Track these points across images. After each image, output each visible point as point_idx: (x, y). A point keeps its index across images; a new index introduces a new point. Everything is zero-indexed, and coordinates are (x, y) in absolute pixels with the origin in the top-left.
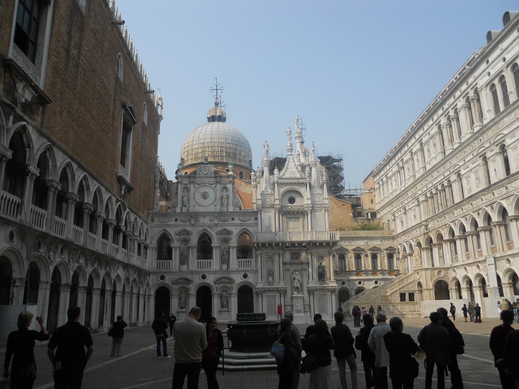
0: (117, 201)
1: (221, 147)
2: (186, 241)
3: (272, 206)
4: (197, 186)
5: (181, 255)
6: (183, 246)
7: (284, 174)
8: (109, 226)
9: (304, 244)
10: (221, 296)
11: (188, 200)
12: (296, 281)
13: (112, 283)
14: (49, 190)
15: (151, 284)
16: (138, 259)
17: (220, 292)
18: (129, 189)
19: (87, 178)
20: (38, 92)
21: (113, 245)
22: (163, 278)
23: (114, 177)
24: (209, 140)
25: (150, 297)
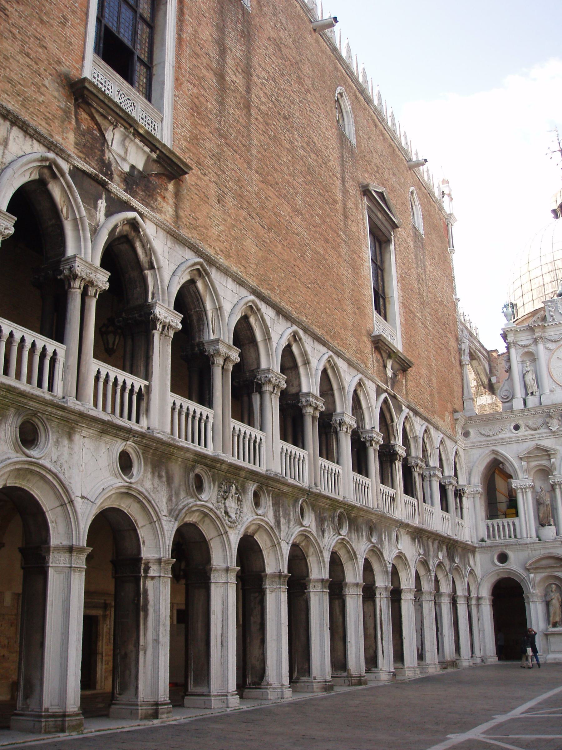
4: (551, 346)
5: (538, 503)
6: (538, 485)
8: (368, 444)
11: (538, 380)
13: (387, 572)
14: (213, 363)
15: (479, 572)
16: (443, 518)
18: (404, 366)
19: (300, 339)
20: (157, 148)
21: (382, 486)
22: (503, 558)
23: (365, 339)
25: (482, 602)
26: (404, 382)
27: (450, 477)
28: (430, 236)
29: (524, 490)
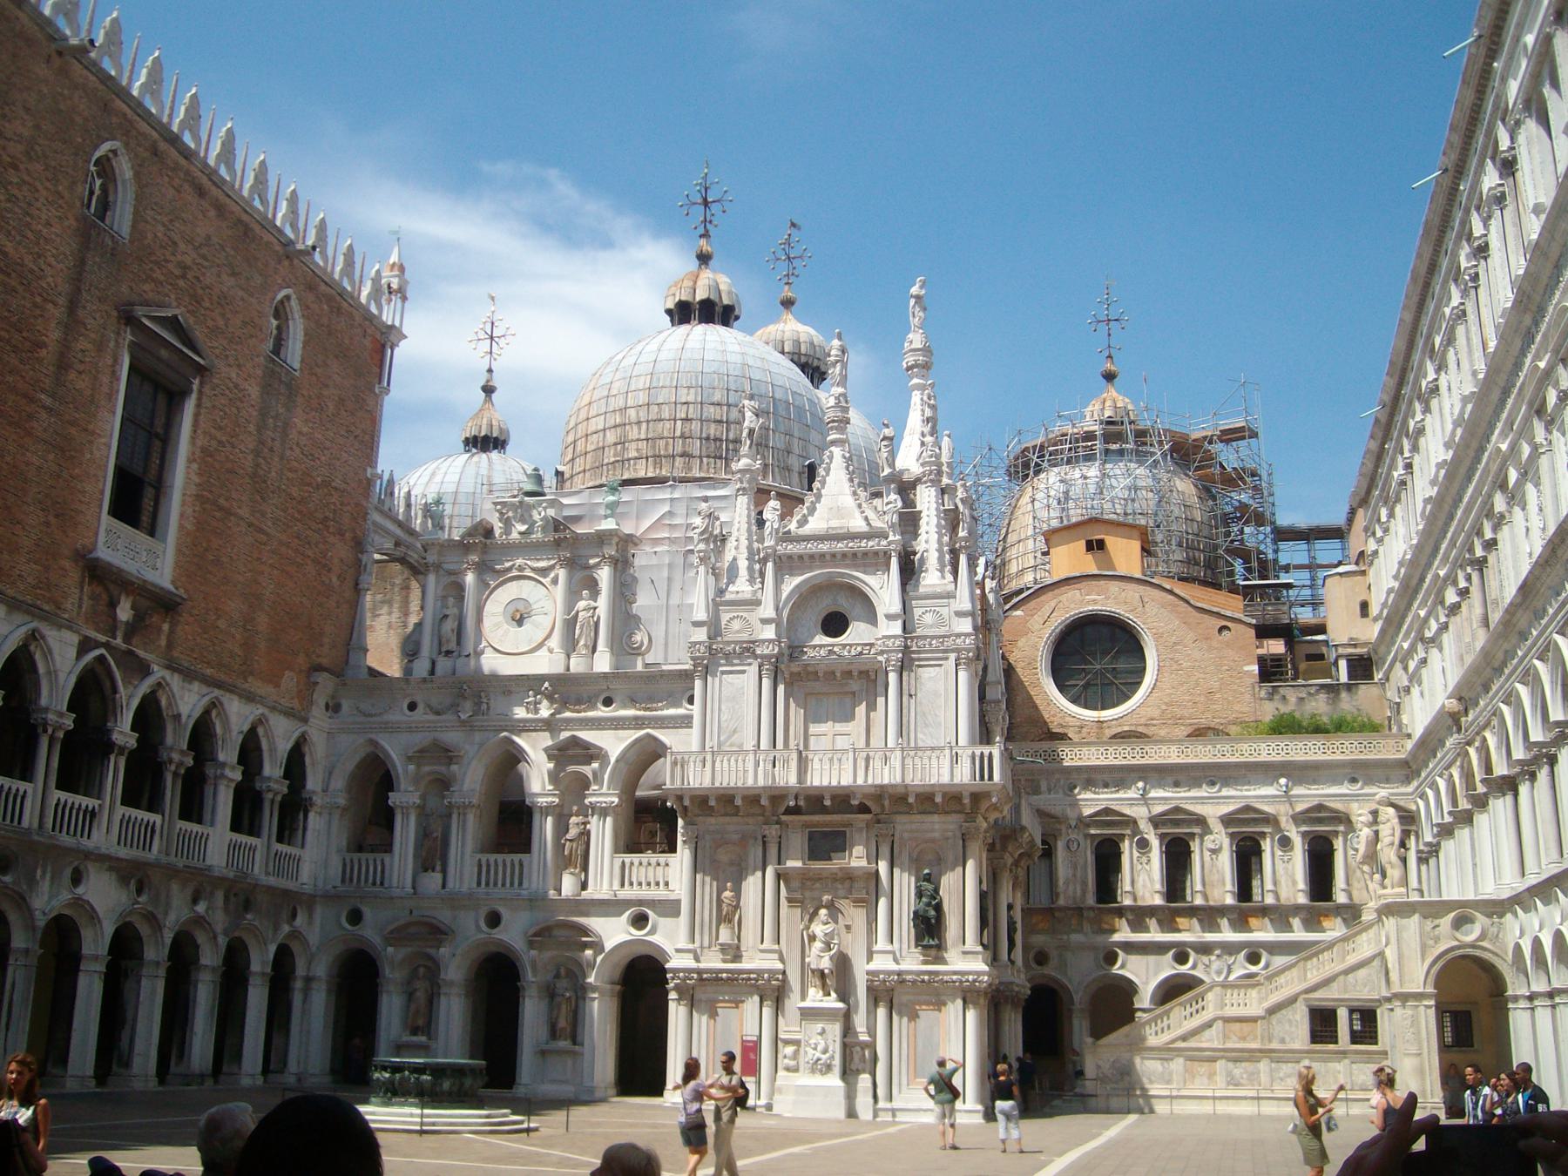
0: (85, 646)
1: (687, 419)
2: (444, 784)
3: (748, 650)
5: (424, 834)
7: (803, 522)
9: (855, 802)
10: (551, 994)
12: (818, 945)
15: (314, 937)
17: (549, 977)
18: (161, 604)
22: (356, 917)
23: (67, 564)
24: (643, 398)
25: (314, 985)
26: (166, 627)
27: (269, 779)
28: (319, 371)
29: (405, 810)
